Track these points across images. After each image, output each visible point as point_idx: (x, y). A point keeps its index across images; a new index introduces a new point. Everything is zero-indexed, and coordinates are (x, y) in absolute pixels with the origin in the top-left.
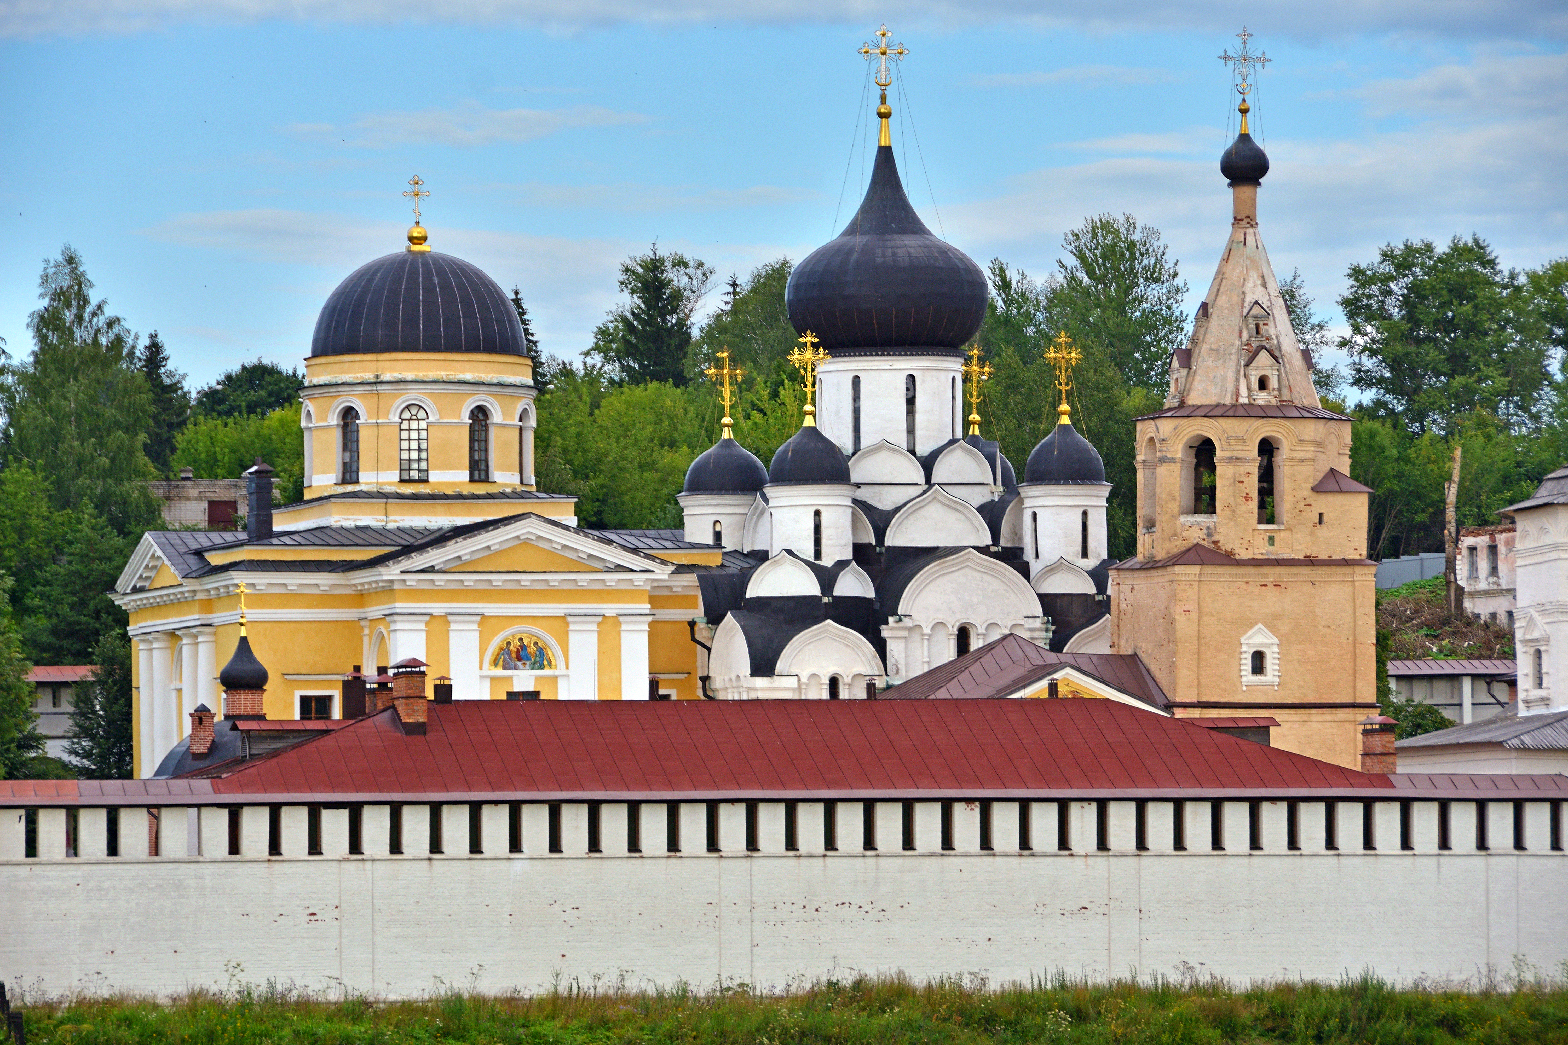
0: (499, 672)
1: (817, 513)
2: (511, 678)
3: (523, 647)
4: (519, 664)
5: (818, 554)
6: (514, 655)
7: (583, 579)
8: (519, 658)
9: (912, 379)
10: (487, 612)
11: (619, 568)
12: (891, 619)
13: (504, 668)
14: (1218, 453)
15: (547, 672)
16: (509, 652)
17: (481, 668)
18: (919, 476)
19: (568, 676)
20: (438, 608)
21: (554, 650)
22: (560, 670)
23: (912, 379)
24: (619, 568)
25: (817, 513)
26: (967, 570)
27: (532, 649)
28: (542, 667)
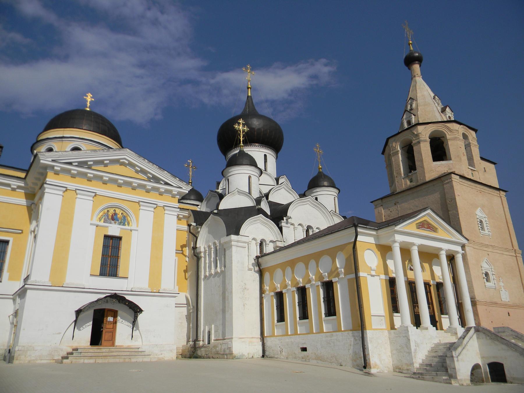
0: (102, 223)
1: (250, 178)
2: (107, 227)
3: (115, 214)
4: (113, 222)
5: (250, 193)
6: (110, 217)
7: (150, 185)
8: (113, 219)
9: (265, 156)
10: (98, 193)
11: (166, 184)
12: (285, 218)
13: (104, 222)
14: (448, 137)
15: (126, 227)
16: (108, 216)
17: (92, 219)
18: (275, 183)
19: (137, 230)
20: (71, 184)
21: (132, 218)
22: (133, 226)
23: (265, 156)
24: (166, 184)
25: (250, 178)
26: (308, 205)
27: (120, 215)
28: (124, 225)
